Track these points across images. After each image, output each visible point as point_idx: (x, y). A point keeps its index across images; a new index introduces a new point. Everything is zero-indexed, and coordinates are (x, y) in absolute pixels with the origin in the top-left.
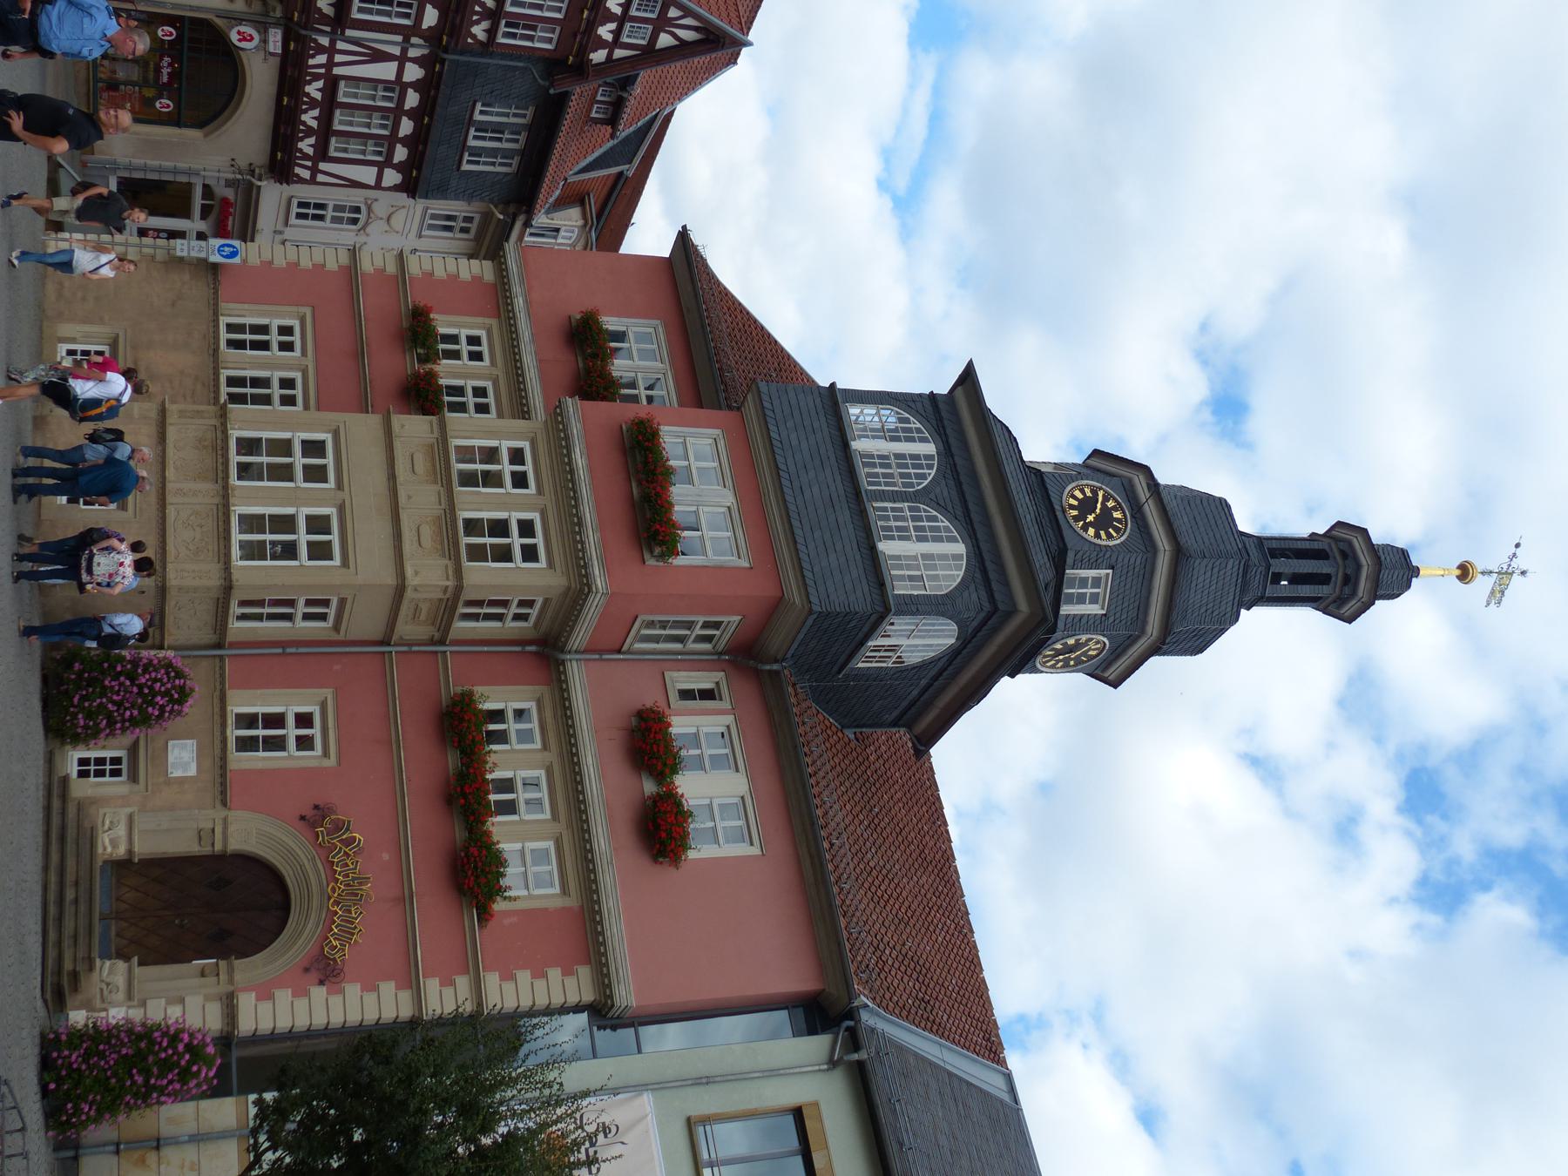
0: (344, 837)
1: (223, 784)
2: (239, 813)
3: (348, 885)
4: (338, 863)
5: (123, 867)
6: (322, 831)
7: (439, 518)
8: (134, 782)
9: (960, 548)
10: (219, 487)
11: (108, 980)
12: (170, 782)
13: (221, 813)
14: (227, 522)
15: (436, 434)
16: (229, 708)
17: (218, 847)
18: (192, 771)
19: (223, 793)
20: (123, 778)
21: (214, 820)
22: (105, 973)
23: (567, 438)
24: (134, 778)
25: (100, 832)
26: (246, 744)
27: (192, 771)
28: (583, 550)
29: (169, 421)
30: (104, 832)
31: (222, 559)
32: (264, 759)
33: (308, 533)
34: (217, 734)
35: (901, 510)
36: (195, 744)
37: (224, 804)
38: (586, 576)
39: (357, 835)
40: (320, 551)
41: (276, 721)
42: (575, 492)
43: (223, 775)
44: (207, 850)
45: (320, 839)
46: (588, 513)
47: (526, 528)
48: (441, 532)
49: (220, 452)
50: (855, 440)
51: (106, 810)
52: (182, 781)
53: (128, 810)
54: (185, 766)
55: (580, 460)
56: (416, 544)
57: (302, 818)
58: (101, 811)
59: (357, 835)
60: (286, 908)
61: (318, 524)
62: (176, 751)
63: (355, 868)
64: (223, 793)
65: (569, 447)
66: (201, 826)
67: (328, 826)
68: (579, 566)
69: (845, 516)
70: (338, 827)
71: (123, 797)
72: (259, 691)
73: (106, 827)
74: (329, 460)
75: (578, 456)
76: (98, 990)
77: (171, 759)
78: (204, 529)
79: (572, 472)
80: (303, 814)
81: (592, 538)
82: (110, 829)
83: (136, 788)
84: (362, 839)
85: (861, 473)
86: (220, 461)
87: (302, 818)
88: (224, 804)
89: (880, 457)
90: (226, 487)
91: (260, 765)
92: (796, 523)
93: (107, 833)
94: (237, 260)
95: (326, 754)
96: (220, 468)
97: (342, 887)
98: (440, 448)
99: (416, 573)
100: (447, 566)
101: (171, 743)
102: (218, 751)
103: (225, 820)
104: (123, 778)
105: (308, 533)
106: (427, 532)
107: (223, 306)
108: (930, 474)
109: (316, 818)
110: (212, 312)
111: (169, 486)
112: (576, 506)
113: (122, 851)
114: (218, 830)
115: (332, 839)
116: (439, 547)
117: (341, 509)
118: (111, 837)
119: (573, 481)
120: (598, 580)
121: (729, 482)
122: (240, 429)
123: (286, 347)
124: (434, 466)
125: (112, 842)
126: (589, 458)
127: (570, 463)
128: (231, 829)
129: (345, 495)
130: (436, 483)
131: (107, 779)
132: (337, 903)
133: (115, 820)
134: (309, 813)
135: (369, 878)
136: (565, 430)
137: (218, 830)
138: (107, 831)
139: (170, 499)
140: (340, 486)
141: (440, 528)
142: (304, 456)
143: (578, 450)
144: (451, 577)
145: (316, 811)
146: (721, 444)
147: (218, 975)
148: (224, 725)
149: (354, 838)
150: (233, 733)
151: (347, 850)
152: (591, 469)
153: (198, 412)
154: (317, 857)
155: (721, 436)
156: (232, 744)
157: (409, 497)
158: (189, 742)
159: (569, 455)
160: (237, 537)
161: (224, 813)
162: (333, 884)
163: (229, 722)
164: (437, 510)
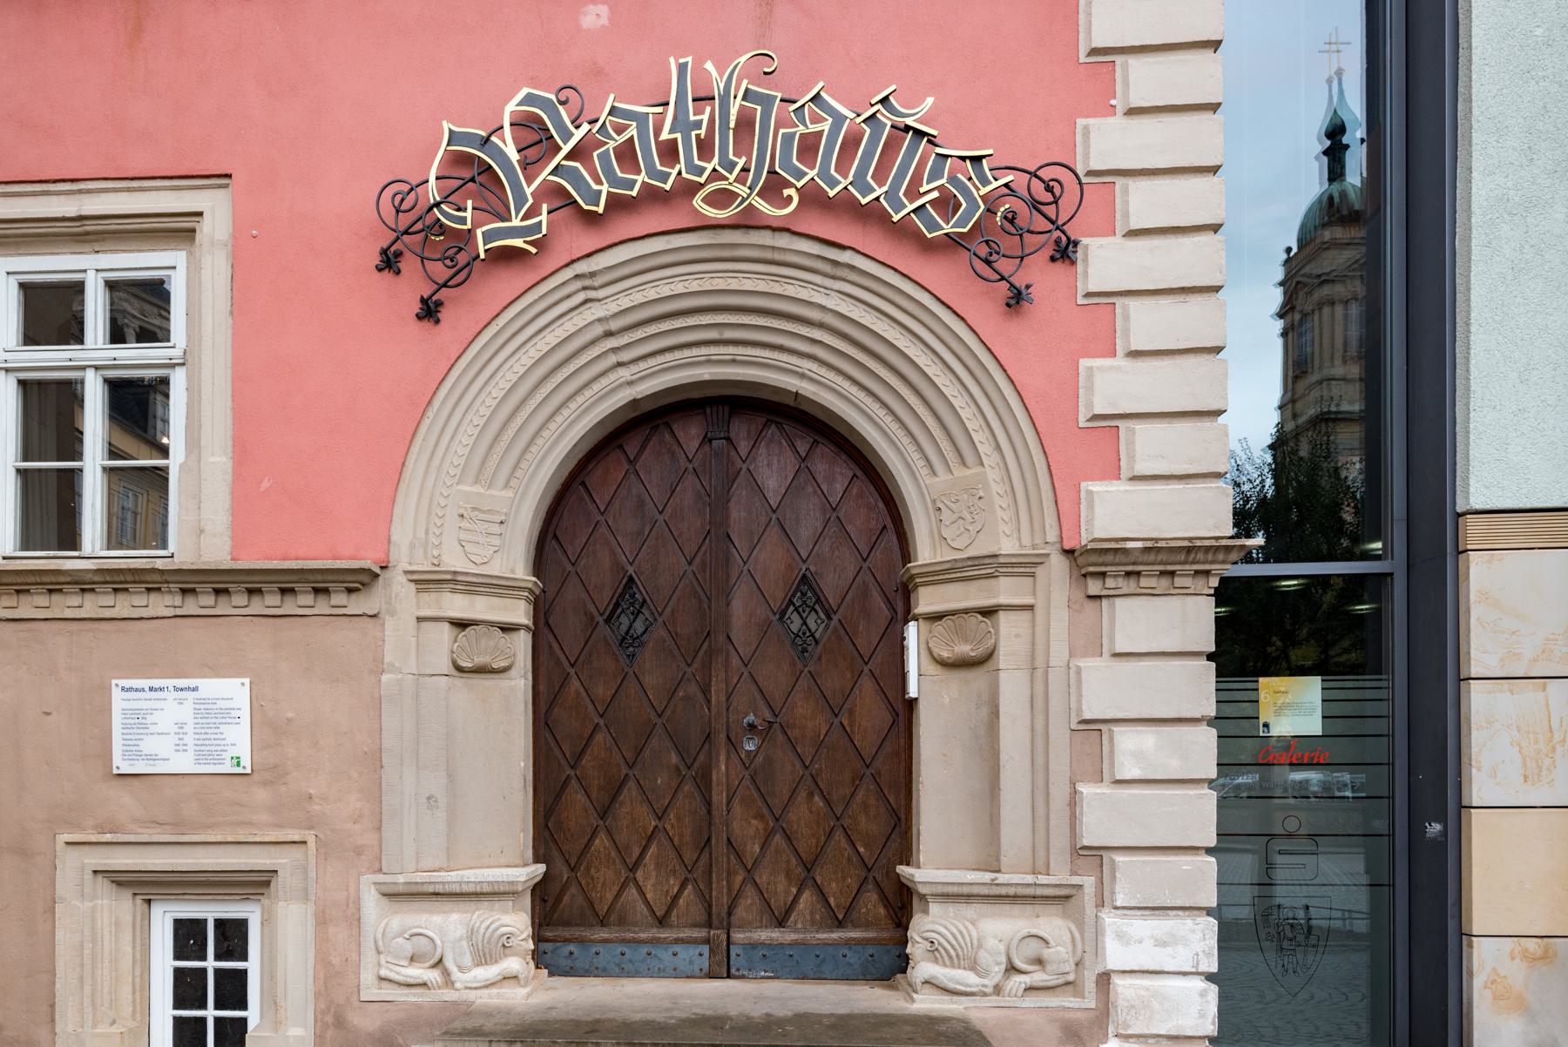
0: (514, 156)
1: (287, 583)
3: (705, 148)
4: (614, 181)
6: (488, 237)
8: (267, 884)
11: (998, 971)
13: (397, 596)
18: (234, 692)
19: (321, 583)
20: (251, 913)
21: (420, 619)
22: (970, 979)
25: (449, 995)
27: (234, 692)
30: (448, 981)
34: (91, 606)
36: (127, 683)
37: (361, 580)
39: (511, 107)
43: (253, 583)
44: (522, 642)
45: (518, 242)
51: (367, 977)
52: (267, 727)
53: (371, 903)
54: (211, 715)
57: (430, 311)
58: (371, 991)
59: (511, 107)
62: (149, 745)
63: (641, 119)
64: (321, 583)
66: (446, 666)
67: (468, 214)
71: (322, 920)
73: (433, 976)
76: (1032, 1001)
77: (183, 763)
80: (416, 307)
83: (285, 881)
84: (525, 91)
87: (430, 311)
88: (361, 580)
93: (456, 975)
97: (709, 167)
101: (121, 764)
103: (426, 582)
104: (251, 913)
113: (517, 922)
114: (459, 606)
115: (520, 198)
118: (467, 960)
131: (253, 966)
133: (408, 948)
134: (412, 285)
135: (682, 69)
137: (459, 606)
138: (446, 973)
145: (409, 264)
147: (989, 612)
148: (54, 584)
149: (523, 123)
151: (566, 149)
154: (583, 267)
158: (119, 701)
161: (397, 587)
162: (697, 202)
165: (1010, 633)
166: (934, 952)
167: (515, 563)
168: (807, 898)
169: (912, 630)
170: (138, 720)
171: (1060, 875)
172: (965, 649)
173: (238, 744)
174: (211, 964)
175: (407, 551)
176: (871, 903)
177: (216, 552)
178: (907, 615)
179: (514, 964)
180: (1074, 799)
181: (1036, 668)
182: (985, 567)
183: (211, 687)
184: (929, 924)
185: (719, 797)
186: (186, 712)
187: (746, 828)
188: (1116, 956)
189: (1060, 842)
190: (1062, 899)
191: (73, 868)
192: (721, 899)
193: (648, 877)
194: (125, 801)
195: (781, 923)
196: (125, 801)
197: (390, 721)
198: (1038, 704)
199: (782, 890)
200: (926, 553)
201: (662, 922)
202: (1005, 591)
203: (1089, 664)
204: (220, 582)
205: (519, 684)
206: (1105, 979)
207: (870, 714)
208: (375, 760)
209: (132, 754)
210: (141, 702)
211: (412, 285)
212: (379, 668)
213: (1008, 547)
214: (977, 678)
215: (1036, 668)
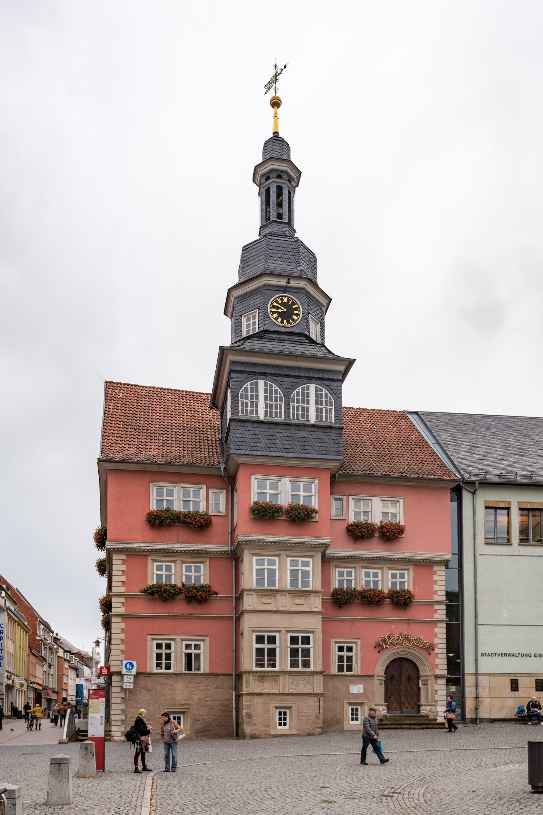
1: (366, 676)
2: (376, 672)
5: (388, 708)
7: (291, 596)
9: (312, 387)
10: (281, 675)
12: (364, 693)
14: (294, 672)
15: (254, 593)
16: (336, 674)
17: (384, 679)
18: (361, 686)
23: (259, 542)
24: (361, 704)
26: (350, 669)
27: (361, 686)
28: (311, 544)
29: (251, 691)
31: (312, 674)
32: (356, 662)
33: (298, 644)
34: (347, 678)
35: (293, 407)
37: (373, 676)
38: (323, 545)
40: (306, 640)
41: (341, 659)
42: (285, 543)
43: (363, 676)
44: (384, 681)
46: (295, 539)
47: (293, 564)
48: (297, 596)
49: (265, 674)
50: (259, 417)
52: (364, 689)
54: (359, 688)
55: (270, 538)
56: (303, 606)
57: (379, 652)
60: (401, 659)
61: (294, 640)
62: (353, 691)
64: (369, 676)
65: (263, 542)
68: (316, 547)
69: (299, 433)
70: (384, 641)
72: (331, 664)
74: (266, 635)
75: (269, 539)
77: (356, 692)
78: (299, 680)
79: (275, 542)
81: (306, 540)
82: (380, 711)
83: (366, 703)
85: (276, 420)
86: (269, 674)
88: (373, 676)
89: (266, 407)
90: (278, 672)
91: (359, 665)
92: (303, 456)
94: (135, 663)
95: (355, 643)
96: (273, 674)
98: (260, 593)
99: (316, 607)
100: (314, 596)
101: (350, 692)
102: (353, 678)
103: (378, 676)
105: (298, 644)
106: (298, 601)
107: (148, 671)
108: (275, 387)
109: (380, 647)
110: (152, 676)
111: (281, 691)
112: (292, 543)
116: (304, 597)
117: (288, 632)
119: (279, 543)
120: (325, 541)
121: (278, 478)
122: (252, 666)
123: (168, 646)
124: (267, 595)
125: (382, 711)
126: (269, 534)
127: (271, 542)
128: (380, 674)
129: (283, 630)
130: (275, 596)
132: (410, 643)
136: (255, 542)
137: (380, 678)
139: (287, 692)
140: (279, 632)
141: (295, 596)
142: (264, 644)
143: (265, 538)
144: (319, 595)
145: (377, 648)
146: (259, 477)
147: (427, 680)
150: (345, 672)
152: (275, 535)
153: (246, 681)
155: (255, 476)
156: (349, 673)
157: (283, 606)
159: (267, 542)
160: (301, 669)
161: (376, 677)
163: (341, 674)
164: (288, 596)
165: (429, 682)
166: (423, 710)
167: (383, 674)
168: (410, 707)
169: (420, 681)
170: (352, 689)
171: (434, 703)
172: (425, 683)
173: (361, 691)
174: (355, 712)
175: (376, 674)
176: (416, 707)
177: (359, 673)
178: (419, 679)
179: (386, 711)
180: (435, 697)
181: (432, 685)
182: (427, 676)
183: (359, 685)
184: (422, 708)
185: (401, 697)
186: (357, 688)
187: (403, 699)
188: (438, 710)
189: (433, 700)
190: (434, 705)
191: (345, 702)
192: (401, 706)
193: (394, 704)
194: (350, 696)
195: (407, 709)
196: (350, 696)
197: (375, 689)
198: (432, 688)
199: (407, 706)
200: (421, 674)
201: (395, 709)
202: (429, 678)
203: (436, 685)
204: (360, 676)
205: (384, 685)
206: (437, 712)
207: (415, 689)
208: (374, 692)
209: (352, 692)
210: (352, 687)
211: (377, 649)
212: (374, 684)
213: (429, 674)
214: (426, 686)
215: (432, 685)
